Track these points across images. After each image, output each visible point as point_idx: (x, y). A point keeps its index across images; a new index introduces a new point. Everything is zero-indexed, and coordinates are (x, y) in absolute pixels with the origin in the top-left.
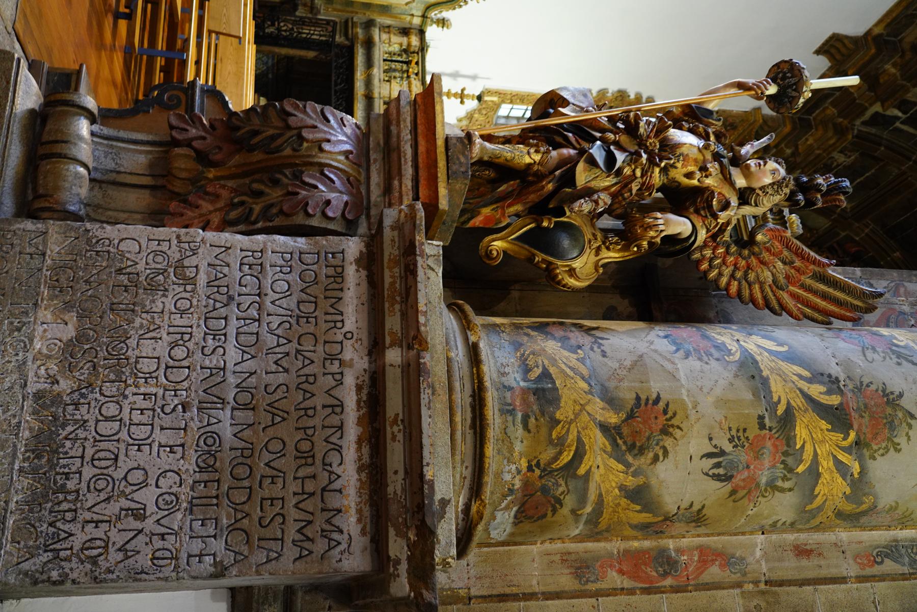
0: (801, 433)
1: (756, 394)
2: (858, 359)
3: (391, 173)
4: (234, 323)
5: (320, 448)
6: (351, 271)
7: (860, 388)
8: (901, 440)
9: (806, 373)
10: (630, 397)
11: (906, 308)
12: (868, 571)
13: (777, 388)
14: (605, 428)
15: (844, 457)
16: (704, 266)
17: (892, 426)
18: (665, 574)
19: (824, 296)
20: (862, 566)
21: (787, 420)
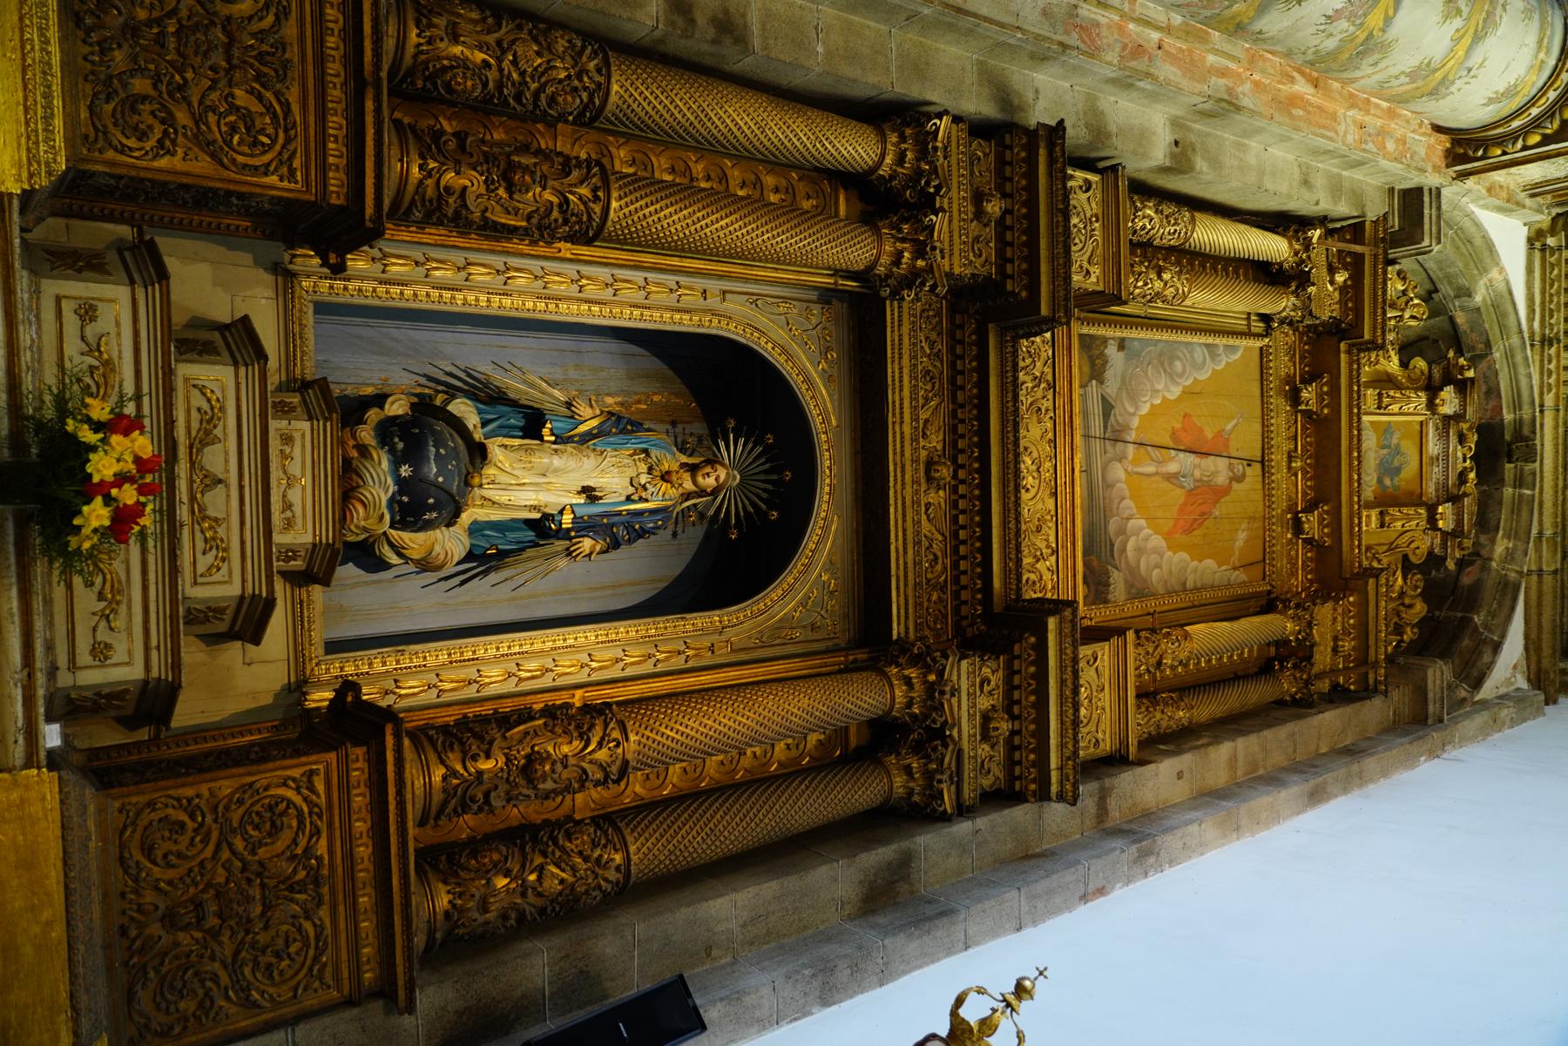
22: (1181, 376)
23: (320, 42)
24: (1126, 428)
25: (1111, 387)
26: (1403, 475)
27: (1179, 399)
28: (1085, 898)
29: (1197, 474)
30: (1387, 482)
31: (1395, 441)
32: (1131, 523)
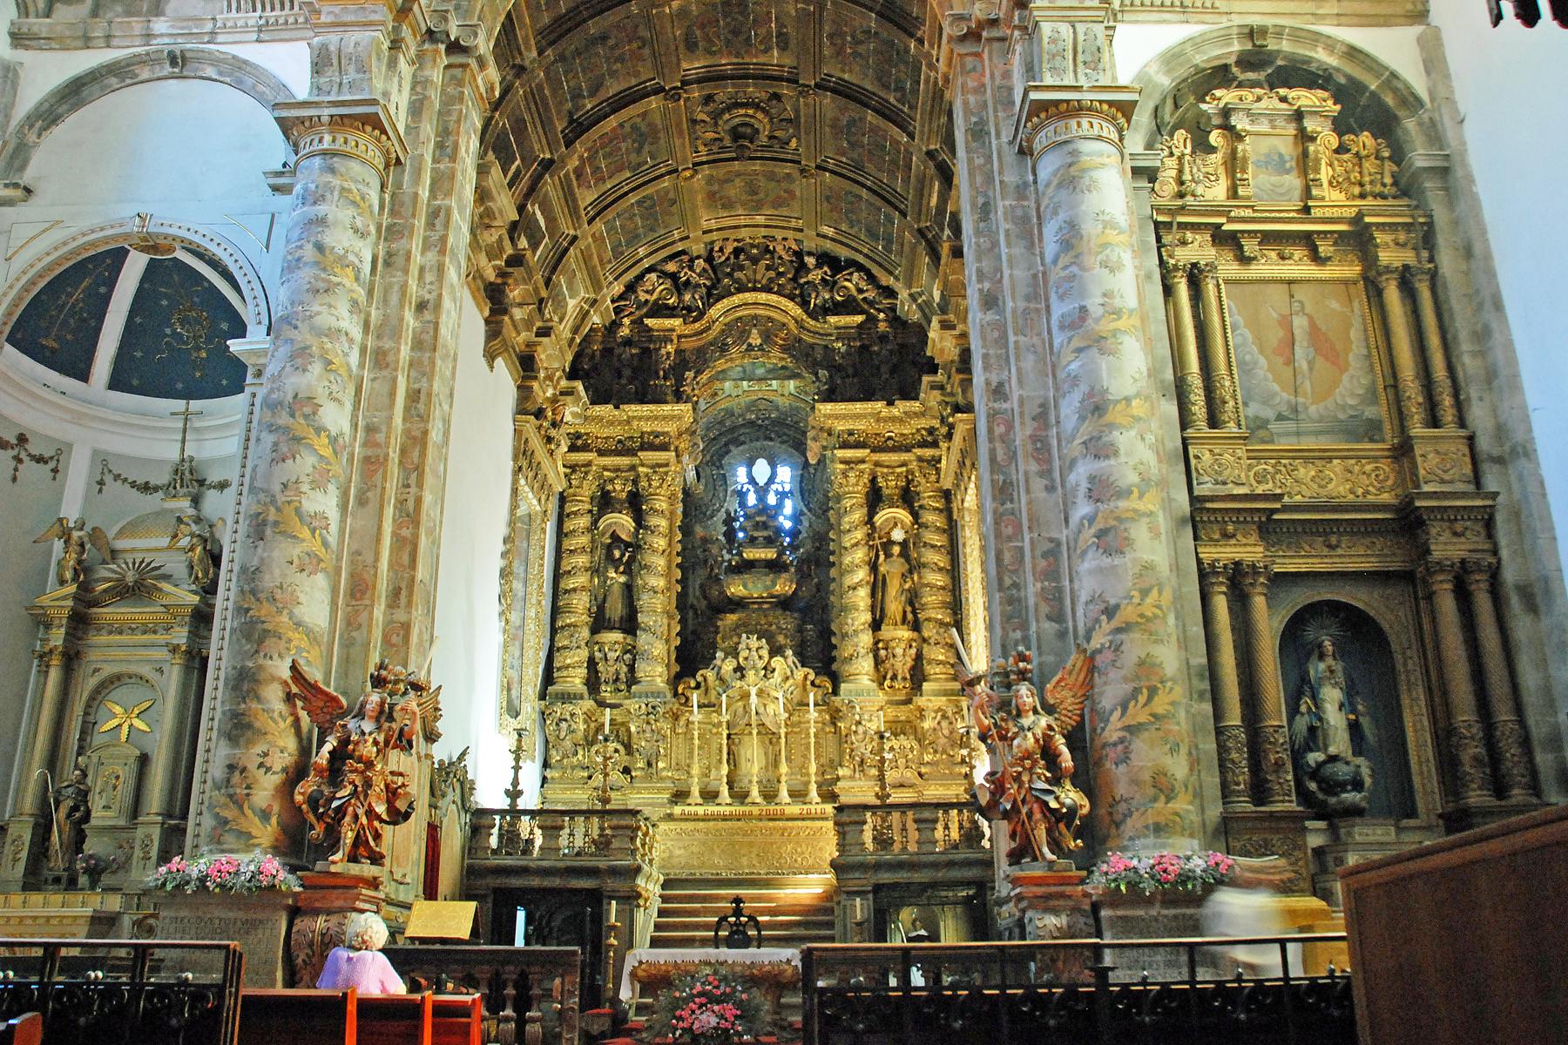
0: (1160, 710)
2: (1123, 672)
3: (1062, 896)
4: (1146, 958)
5: (1191, 923)
6: (1119, 913)
7: (1138, 678)
8: (1158, 661)
10: (1153, 790)
11: (1039, 585)
13: (1143, 718)
15: (1167, 690)
19: (1078, 674)
21: (1154, 716)
22: (1252, 355)
24: (1289, 402)
25: (1269, 413)
26: (1283, 150)
27: (1266, 357)
28: (1544, 495)
29: (1305, 344)
30: (1288, 165)
31: (1262, 158)
32: (1339, 402)
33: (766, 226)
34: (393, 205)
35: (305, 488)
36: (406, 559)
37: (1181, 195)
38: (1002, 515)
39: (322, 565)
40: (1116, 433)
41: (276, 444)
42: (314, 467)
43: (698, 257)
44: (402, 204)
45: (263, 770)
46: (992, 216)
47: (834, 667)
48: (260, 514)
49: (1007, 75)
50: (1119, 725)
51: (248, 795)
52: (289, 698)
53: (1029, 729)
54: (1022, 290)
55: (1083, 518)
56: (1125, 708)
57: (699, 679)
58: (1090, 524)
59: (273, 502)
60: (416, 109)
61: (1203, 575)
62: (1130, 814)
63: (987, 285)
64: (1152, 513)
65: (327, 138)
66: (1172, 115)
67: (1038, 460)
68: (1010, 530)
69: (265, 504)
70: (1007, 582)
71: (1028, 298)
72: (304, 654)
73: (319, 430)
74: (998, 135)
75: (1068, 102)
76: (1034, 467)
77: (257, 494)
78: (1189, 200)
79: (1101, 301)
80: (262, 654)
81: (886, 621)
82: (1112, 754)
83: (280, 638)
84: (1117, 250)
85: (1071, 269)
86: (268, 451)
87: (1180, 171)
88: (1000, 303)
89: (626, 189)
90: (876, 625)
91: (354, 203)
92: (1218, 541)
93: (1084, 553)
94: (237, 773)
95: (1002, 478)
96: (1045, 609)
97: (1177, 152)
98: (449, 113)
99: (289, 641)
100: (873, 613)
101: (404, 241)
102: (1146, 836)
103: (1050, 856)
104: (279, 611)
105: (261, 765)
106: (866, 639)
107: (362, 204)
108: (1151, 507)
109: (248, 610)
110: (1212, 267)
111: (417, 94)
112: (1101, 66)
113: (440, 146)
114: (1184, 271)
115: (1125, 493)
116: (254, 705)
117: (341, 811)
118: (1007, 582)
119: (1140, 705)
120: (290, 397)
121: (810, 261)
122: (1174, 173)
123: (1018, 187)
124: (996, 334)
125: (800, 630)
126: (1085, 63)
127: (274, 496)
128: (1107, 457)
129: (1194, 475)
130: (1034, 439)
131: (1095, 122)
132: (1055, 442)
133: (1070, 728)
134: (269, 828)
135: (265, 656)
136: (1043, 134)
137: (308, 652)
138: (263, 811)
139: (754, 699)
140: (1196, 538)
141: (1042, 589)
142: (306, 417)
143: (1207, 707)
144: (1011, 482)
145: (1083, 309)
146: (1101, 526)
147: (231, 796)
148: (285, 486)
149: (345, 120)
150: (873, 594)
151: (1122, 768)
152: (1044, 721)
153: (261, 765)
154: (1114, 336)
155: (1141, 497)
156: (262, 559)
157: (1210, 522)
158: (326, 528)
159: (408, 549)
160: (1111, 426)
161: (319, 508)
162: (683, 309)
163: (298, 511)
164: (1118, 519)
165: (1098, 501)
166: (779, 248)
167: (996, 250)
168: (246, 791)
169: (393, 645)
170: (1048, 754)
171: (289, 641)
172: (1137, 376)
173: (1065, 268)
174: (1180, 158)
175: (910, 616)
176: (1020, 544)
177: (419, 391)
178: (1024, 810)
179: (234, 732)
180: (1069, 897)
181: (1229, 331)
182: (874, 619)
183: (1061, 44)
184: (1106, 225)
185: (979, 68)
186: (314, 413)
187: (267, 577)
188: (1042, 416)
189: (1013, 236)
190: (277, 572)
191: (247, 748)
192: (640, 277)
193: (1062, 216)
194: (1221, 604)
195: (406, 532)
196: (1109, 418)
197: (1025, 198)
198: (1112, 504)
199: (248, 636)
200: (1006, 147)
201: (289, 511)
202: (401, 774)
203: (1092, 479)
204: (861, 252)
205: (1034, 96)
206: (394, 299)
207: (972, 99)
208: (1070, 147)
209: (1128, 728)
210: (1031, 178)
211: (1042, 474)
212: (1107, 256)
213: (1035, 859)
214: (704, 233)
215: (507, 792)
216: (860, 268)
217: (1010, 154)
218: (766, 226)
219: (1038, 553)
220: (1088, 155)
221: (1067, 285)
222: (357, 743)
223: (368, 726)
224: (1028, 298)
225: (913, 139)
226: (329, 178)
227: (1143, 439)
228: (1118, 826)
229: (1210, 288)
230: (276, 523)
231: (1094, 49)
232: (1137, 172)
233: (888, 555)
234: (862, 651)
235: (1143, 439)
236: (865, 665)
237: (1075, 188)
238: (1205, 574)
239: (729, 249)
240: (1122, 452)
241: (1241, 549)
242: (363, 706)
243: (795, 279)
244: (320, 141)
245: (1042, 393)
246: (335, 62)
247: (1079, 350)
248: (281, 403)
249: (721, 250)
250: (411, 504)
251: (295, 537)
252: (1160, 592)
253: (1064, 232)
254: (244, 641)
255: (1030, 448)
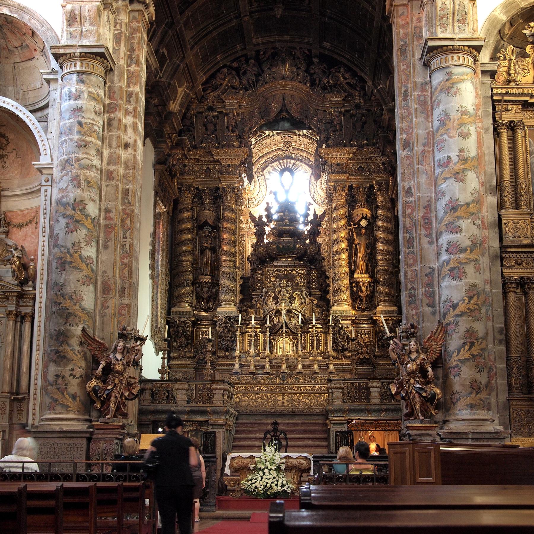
0: (475, 353)
1: (468, 361)
8: (476, 329)
9: (463, 349)
10: (470, 389)
11: (424, 290)
12: (491, 319)
13: (467, 356)
14: (476, 395)
16: (432, 360)
17: (473, 332)
18: (493, 370)
19: (439, 334)
20: (490, 320)
21: (473, 356)
23: (525, 405)
33: (291, 42)
34: (110, 93)
35: (83, 245)
36: (127, 274)
37: (509, 82)
38: (408, 254)
39: (92, 281)
40: (461, 221)
41: (67, 224)
42: (86, 235)
43: (251, 58)
44: (114, 92)
45: (72, 377)
46: (409, 98)
47: (328, 296)
48: (62, 258)
49: (419, 20)
50: (456, 359)
51: (66, 388)
52: (81, 344)
53: (414, 360)
54: (422, 141)
55: (444, 261)
56: (459, 352)
57: (254, 303)
58: (447, 264)
59: (69, 252)
60: (117, 39)
61: (504, 285)
62: (460, 399)
63: (405, 136)
64: (476, 260)
65: (78, 64)
66: (509, 30)
67: (426, 229)
68: (412, 261)
69: (64, 253)
70: (410, 286)
71: (424, 145)
72: (87, 323)
73: (87, 216)
74: (413, 56)
75: (447, 46)
76: (423, 232)
77: (60, 248)
78: (513, 84)
79: (458, 154)
80: (68, 324)
81: (357, 271)
82: (453, 372)
83: (76, 316)
84: (467, 126)
85: (444, 136)
86: (64, 227)
87: (509, 68)
88: (411, 145)
89: (211, 28)
90: (352, 273)
91: (95, 99)
92: (513, 266)
93: (444, 277)
94: (60, 378)
95: (408, 235)
96: (426, 301)
97: (508, 57)
98: (133, 38)
99: (80, 317)
100: (350, 268)
101: (117, 113)
102: (467, 410)
103: (422, 418)
104: (75, 304)
105: (71, 375)
106: (345, 282)
107: (98, 99)
108: (476, 257)
109: (60, 304)
110: (521, 122)
111: (117, 30)
112: (466, 22)
113: (130, 57)
114: (506, 125)
115: (463, 250)
116: (67, 347)
117: (109, 395)
118: (410, 286)
119: (466, 350)
120: (72, 201)
121: (316, 60)
122: (505, 69)
123: (422, 84)
124: (408, 162)
125: (309, 274)
126: (458, 20)
127: (68, 249)
128: (456, 233)
129: (504, 232)
130: (424, 218)
131: (461, 56)
132: (434, 220)
133: (434, 359)
134: (76, 403)
135: (70, 324)
136: (435, 60)
137: (88, 322)
138: (73, 395)
139: (284, 316)
140: (502, 265)
141: (425, 291)
142: (80, 210)
143: (503, 348)
144: (413, 238)
145: (449, 157)
146: (452, 266)
147: (58, 389)
148: (73, 244)
149: (88, 55)
150: (350, 257)
151: (457, 378)
152: (422, 356)
153: (71, 375)
154: (463, 172)
155: (471, 252)
156: (65, 280)
157: (511, 257)
158: (92, 263)
159: (127, 269)
160: (459, 218)
161: (89, 254)
162: (242, 89)
163: (80, 256)
164: (460, 263)
165: (451, 254)
166: (298, 53)
167: (410, 117)
168: (65, 387)
169: (123, 315)
170: (423, 371)
171: (80, 317)
172: (473, 192)
173: (442, 135)
174: (510, 60)
175: (370, 269)
176: (416, 268)
177: (128, 190)
178: (411, 396)
179: (57, 360)
180: (431, 435)
181: (529, 156)
182: (350, 270)
183: (446, 11)
184: (463, 113)
185: (406, 13)
186: (84, 208)
187: (68, 288)
188: (428, 207)
189: (418, 113)
190: (73, 286)
191: (65, 367)
192: (218, 70)
193: (442, 108)
194: (512, 299)
195: (126, 261)
196: (458, 213)
197: (425, 90)
198: (457, 256)
199: (61, 316)
200: (417, 62)
201: (76, 256)
202: (134, 378)
203: (449, 243)
204: (346, 58)
205: (430, 44)
206: (114, 144)
207: (401, 31)
208: (447, 70)
209: (459, 360)
210: (429, 79)
211: (427, 236)
212: (462, 130)
213: (415, 418)
214: (255, 45)
215: (159, 371)
216: (345, 65)
217: (419, 66)
218: (291, 42)
219: (424, 274)
220: (456, 75)
221: (441, 144)
222: (114, 365)
223: (119, 356)
224: (424, 145)
225: (375, 10)
226: (81, 86)
227: (474, 223)
228: (454, 405)
229: (520, 134)
230: (71, 263)
231: (463, 13)
232: (483, 72)
233: (359, 234)
234: (344, 289)
235: (474, 223)
236: (346, 296)
237: (448, 93)
238: (506, 283)
239: (269, 53)
240: (463, 230)
241: (525, 271)
242: (116, 348)
243: (307, 71)
244: (75, 66)
245: (429, 194)
246: (78, 19)
247: (446, 179)
248: (68, 203)
249: (264, 53)
250: (127, 247)
251: (79, 269)
252: (478, 298)
253: (442, 116)
254: (59, 318)
255: (422, 222)
